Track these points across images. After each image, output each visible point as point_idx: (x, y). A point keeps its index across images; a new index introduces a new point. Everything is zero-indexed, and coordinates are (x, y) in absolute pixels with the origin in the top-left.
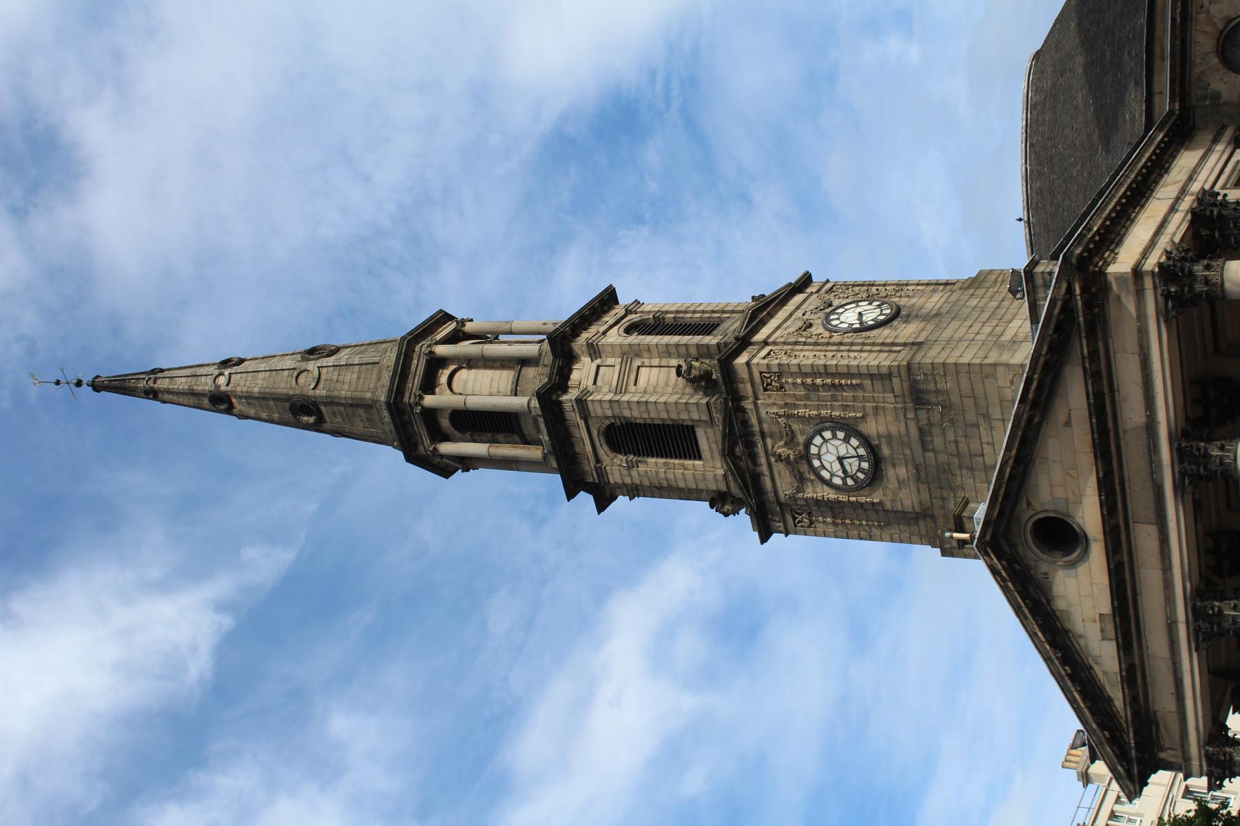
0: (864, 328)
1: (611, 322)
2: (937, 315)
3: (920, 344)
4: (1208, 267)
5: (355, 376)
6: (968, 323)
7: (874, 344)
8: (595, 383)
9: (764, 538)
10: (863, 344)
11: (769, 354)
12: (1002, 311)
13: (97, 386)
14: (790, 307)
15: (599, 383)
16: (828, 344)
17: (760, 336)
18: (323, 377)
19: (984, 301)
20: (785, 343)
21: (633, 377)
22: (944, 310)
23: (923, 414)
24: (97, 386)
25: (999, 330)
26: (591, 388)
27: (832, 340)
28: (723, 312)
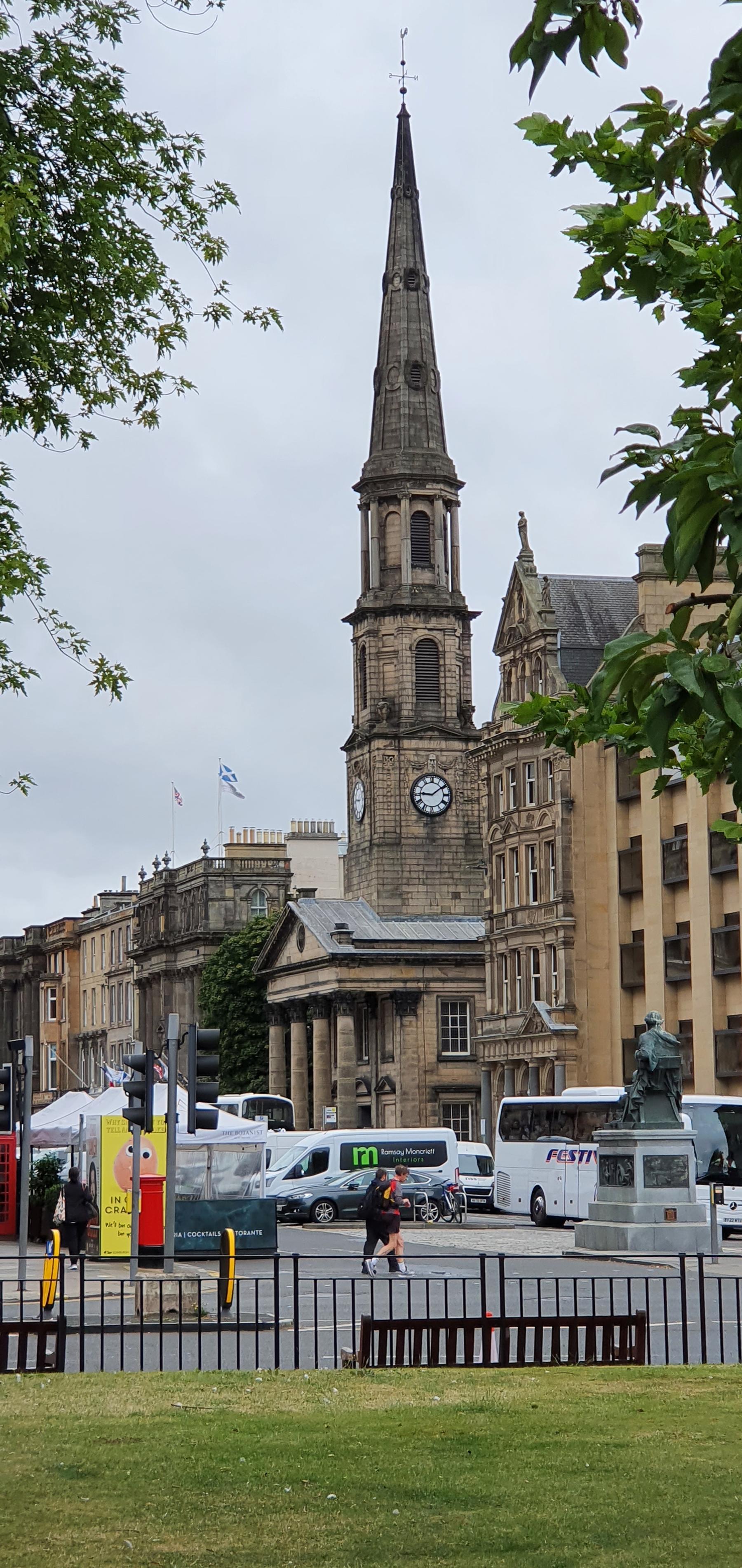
0: (415, 805)
1: (429, 626)
2: (434, 840)
3: (398, 844)
4: (344, 1010)
5: (394, 427)
6: (422, 862)
7: (400, 815)
8: (384, 635)
9: (342, 749)
10: (400, 809)
11: (389, 756)
12: (438, 876)
13: (403, 117)
14: (443, 744)
15: (385, 638)
16: (400, 788)
17: (406, 743)
18: (394, 395)
19: (451, 861)
20: (399, 761)
21: (388, 661)
22: (439, 842)
23: (367, 851)
24: (403, 117)
25: (417, 881)
26: (380, 634)
27: (402, 790)
28: (445, 698)
